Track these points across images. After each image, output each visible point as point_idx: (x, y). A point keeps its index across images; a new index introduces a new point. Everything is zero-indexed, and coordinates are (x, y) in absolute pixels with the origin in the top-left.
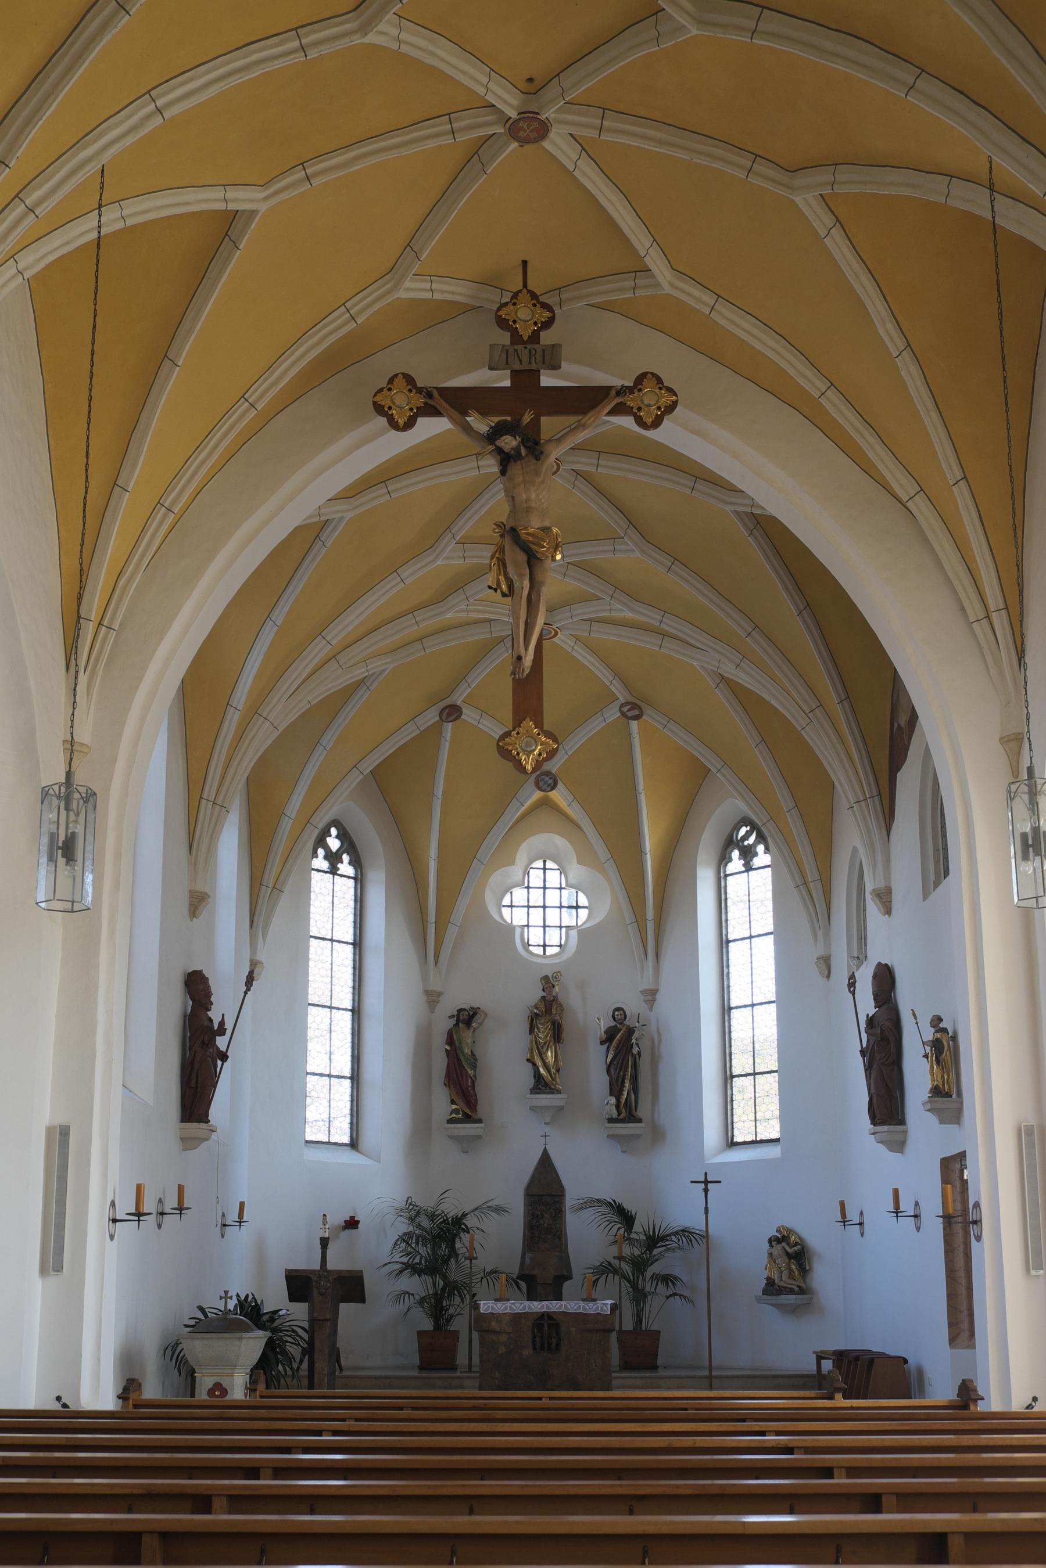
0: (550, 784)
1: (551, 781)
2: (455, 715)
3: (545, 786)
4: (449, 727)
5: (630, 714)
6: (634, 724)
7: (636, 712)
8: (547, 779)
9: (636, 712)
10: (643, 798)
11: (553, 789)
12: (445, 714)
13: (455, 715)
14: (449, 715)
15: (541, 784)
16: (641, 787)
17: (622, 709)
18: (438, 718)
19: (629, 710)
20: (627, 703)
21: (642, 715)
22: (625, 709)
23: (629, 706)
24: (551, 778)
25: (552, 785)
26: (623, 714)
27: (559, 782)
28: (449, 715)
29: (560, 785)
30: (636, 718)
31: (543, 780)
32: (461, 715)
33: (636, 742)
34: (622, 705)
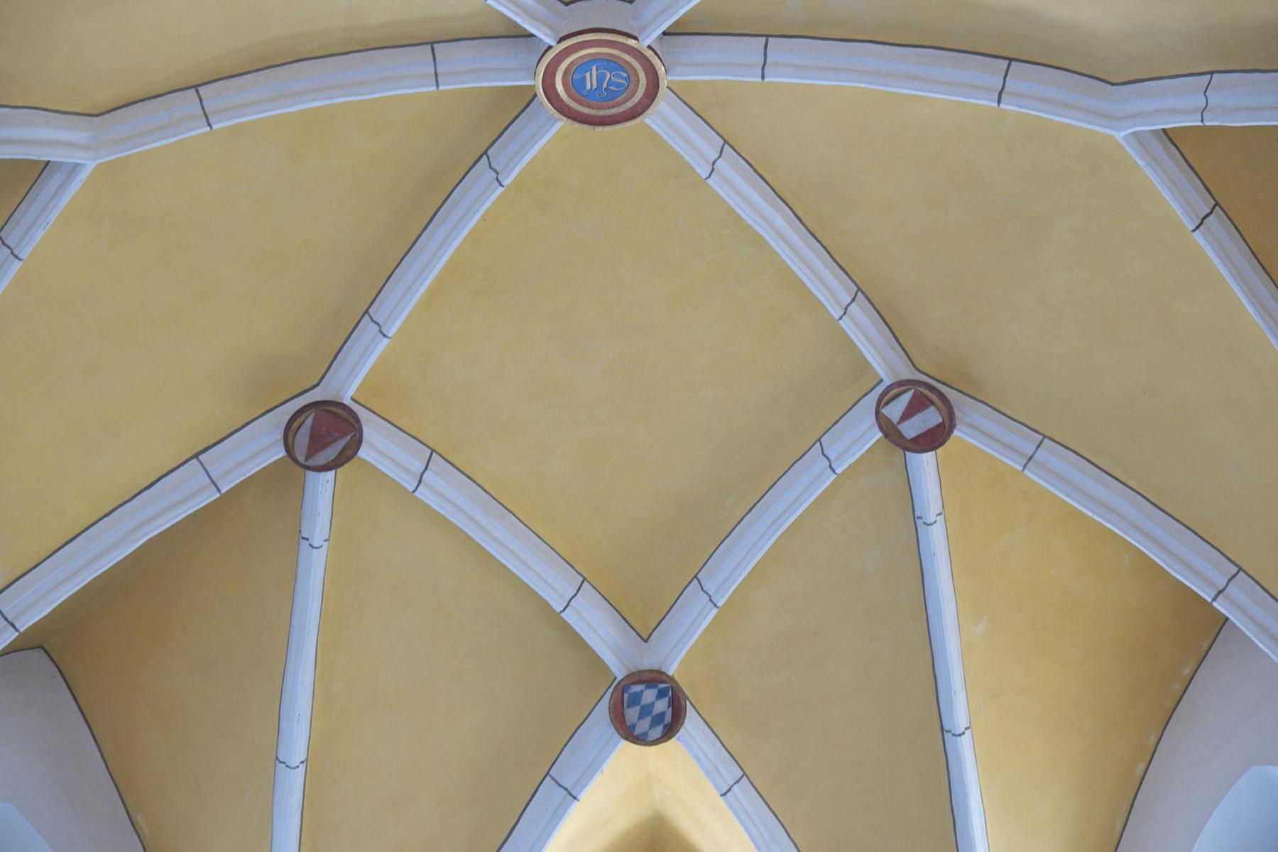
0: (662, 715)
1: (662, 706)
2: (340, 445)
3: (643, 726)
4: (322, 486)
5: (911, 429)
6: (925, 464)
7: (930, 418)
8: (649, 695)
9: (930, 418)
10: (967, 752)
11: (670, 731)
12: (302, 440)
13: (340, 445)
14: (318, 441)
15: (632, 714)
16: (960, 713)
17: (885, 411)
18: (283, 453)
19: (908, 414)
20: (904, 384)
21: (952, 426)
22: (894, 411)
23: (907, 397)
24: (661, 695)
25: (668, 719)
26: (889, 431)
27: (690, 714)
28: (318, 441)
29: (691, 722)
30: (932, 440)
31: (636, 699)
32: (357, 443)
33: (936, 539)
34: (883, 401)
